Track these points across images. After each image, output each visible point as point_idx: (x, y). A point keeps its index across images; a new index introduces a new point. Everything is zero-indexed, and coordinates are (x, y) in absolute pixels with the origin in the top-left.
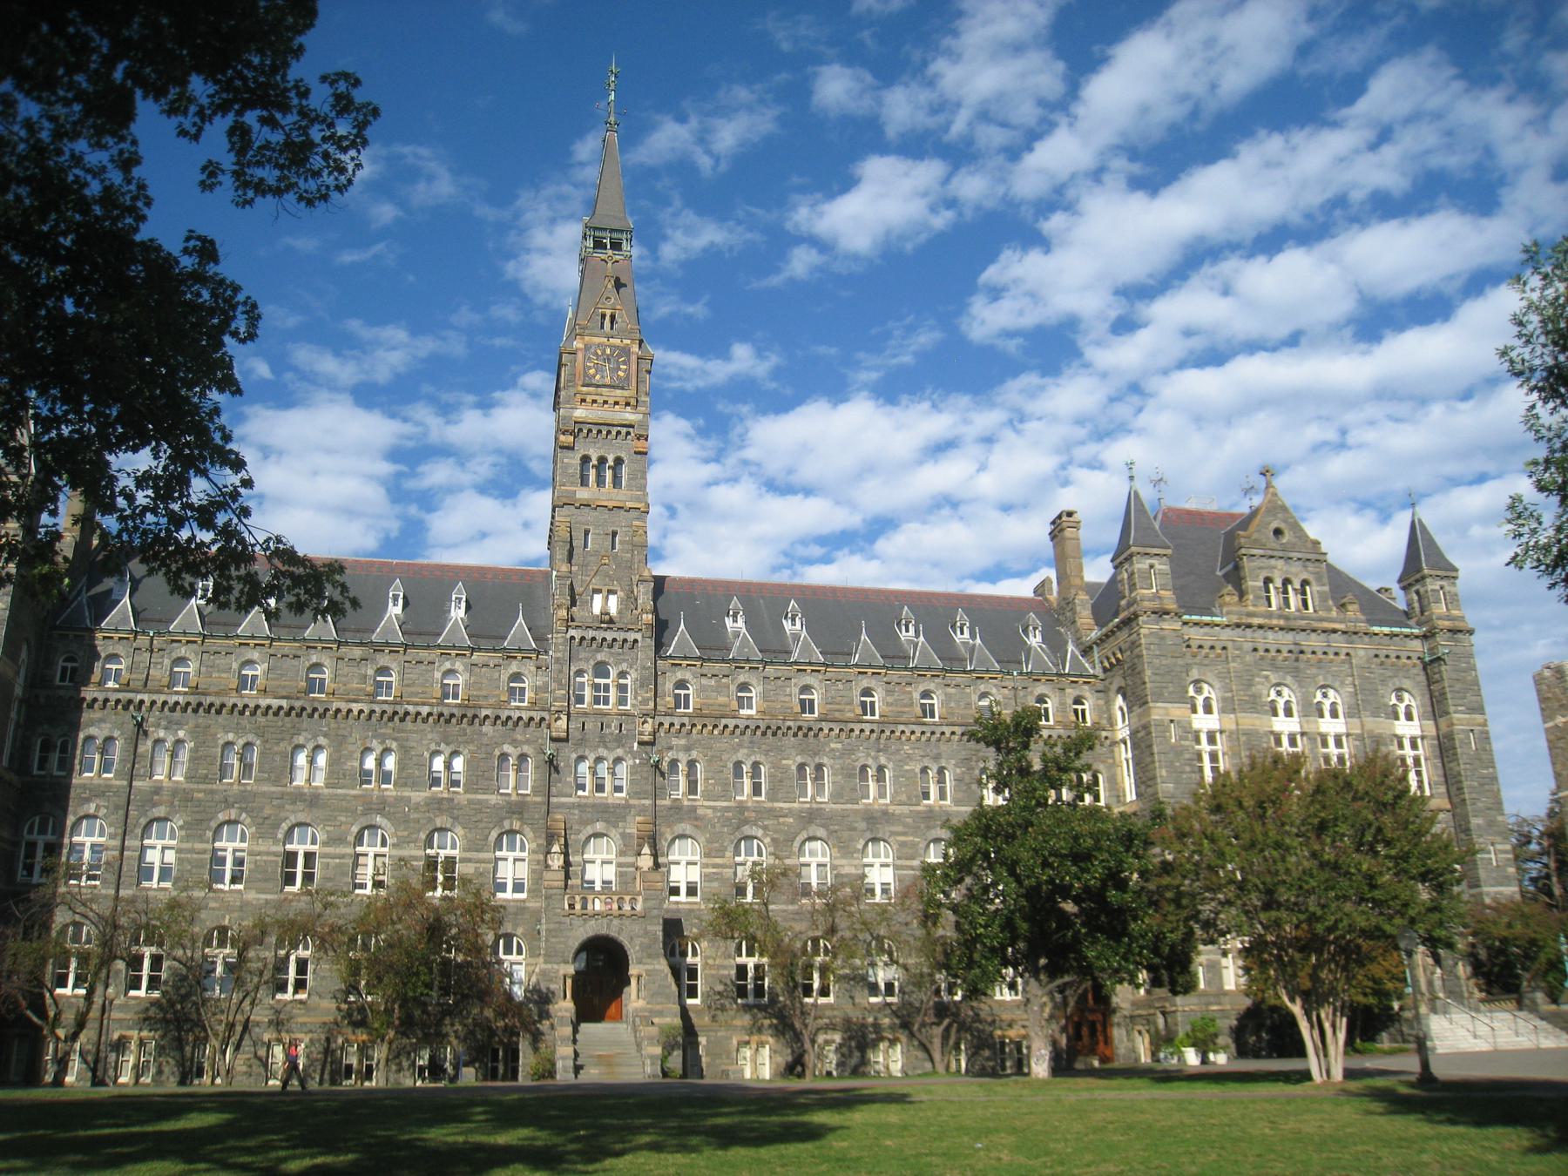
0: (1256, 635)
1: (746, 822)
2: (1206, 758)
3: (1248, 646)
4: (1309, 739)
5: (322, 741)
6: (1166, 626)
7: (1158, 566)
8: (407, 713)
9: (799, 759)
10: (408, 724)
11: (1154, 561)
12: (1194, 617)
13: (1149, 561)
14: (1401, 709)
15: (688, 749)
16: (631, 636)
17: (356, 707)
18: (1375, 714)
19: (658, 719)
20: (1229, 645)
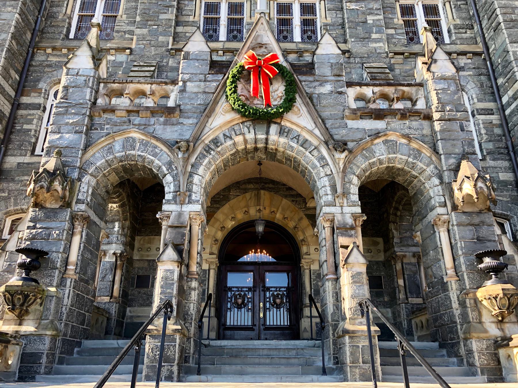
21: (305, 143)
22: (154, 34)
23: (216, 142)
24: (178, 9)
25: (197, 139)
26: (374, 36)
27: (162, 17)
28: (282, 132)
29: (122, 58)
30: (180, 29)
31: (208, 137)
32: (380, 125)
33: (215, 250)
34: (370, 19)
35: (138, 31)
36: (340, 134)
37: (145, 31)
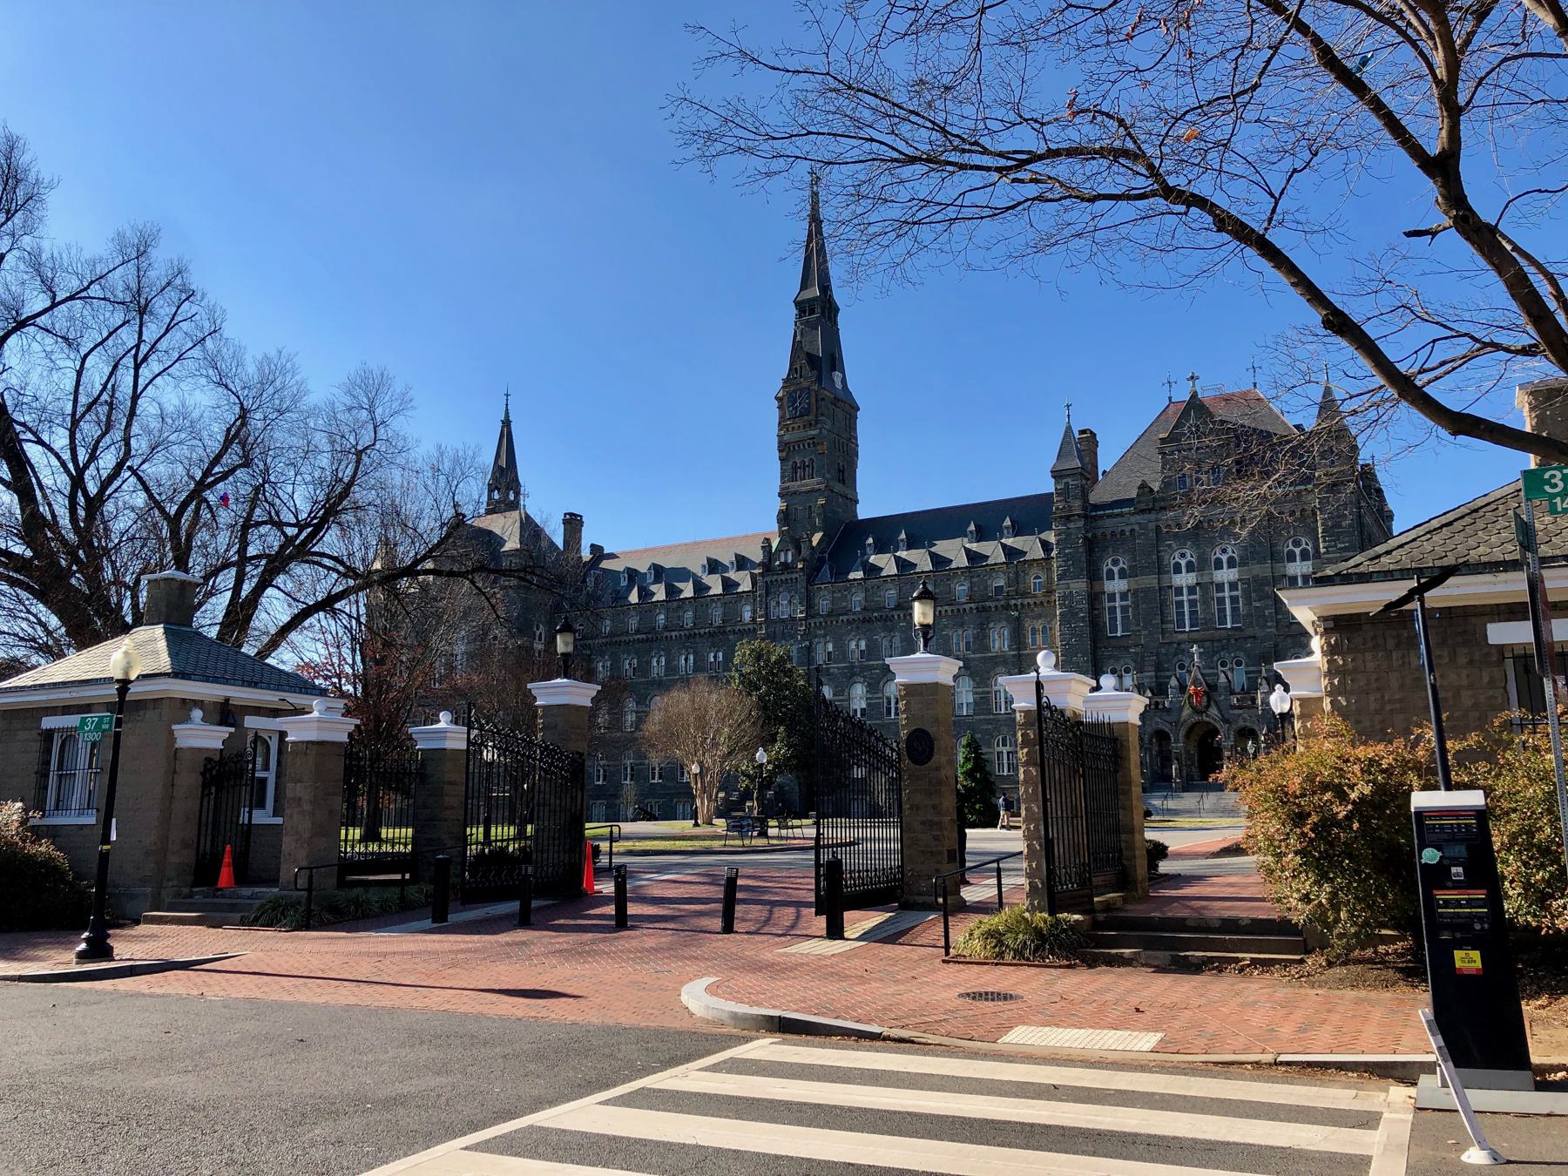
0: (1160, 515)
1: (853, 675)
2: (1118, 610)
3: (1152, 526)
4: (1201, 588)
5: (662, 653)
6: (1072, 525)
7: (1071, 483)
8: (695, 634)
9: (882, 635)
10: (697, 640)
11: (1069, 480)
12: (1107, 512)
13: (1065, 480)
14: (1297, 551)
15: (824, 636)
16: (794, 576)
17: (673, 634)
18: (1262, 561)
19: (809, 621)
20: (1136, 527)
21: (1215, 720)
22: (1151, 633)
23: (1185, 721)
24: (1162, 613)
25: (1179, 721)
26: (1269, 624)
27: (1154, 622)
28: (1208, 716)
29: (1138, 650)
30: (1164, 626)
31: (1182, 720)
32: (1241, 711)
33: (1196, 744)
34: (1267, 612)
35: (1143, 633)
36: (1226, 716)
37: (1146, 632)
